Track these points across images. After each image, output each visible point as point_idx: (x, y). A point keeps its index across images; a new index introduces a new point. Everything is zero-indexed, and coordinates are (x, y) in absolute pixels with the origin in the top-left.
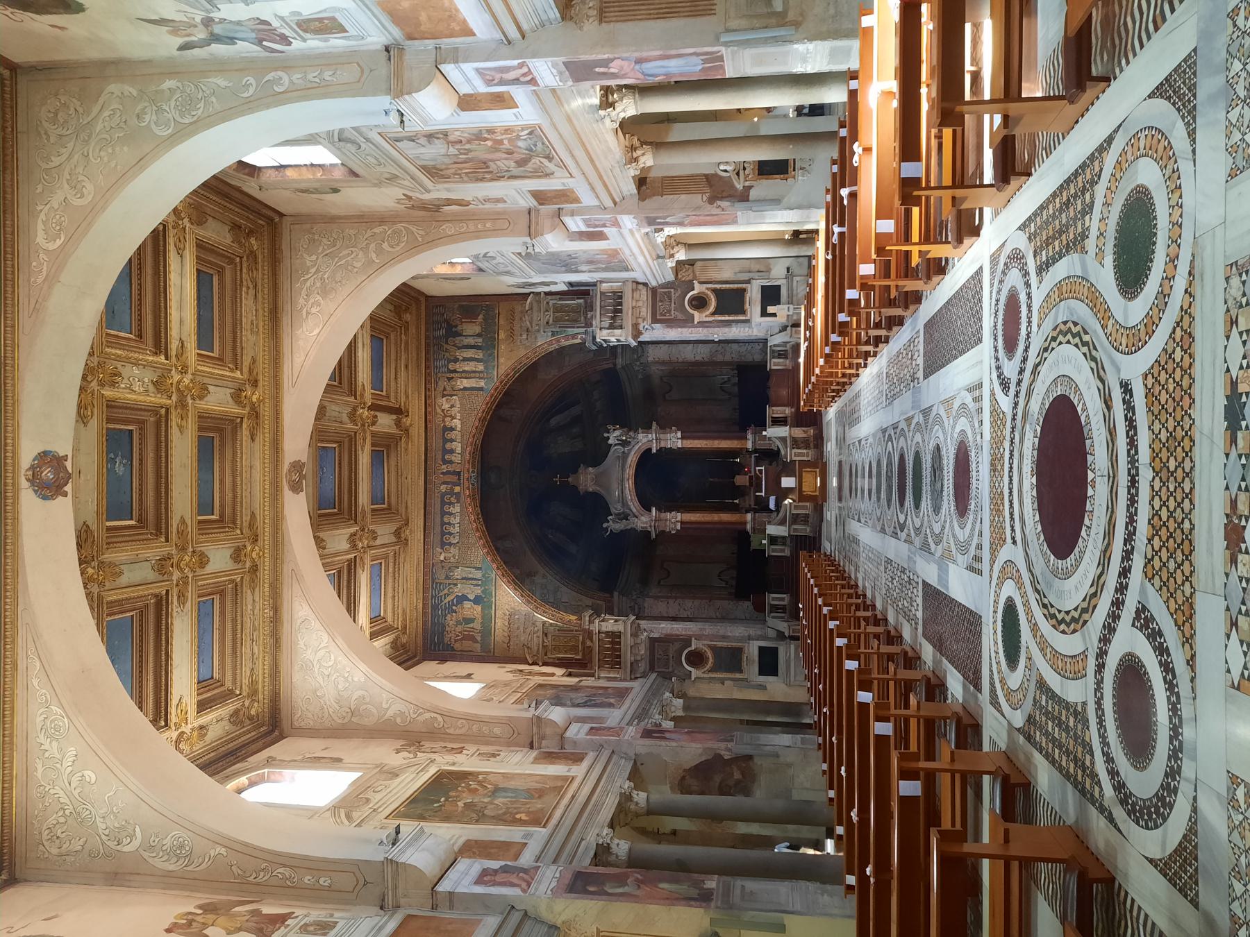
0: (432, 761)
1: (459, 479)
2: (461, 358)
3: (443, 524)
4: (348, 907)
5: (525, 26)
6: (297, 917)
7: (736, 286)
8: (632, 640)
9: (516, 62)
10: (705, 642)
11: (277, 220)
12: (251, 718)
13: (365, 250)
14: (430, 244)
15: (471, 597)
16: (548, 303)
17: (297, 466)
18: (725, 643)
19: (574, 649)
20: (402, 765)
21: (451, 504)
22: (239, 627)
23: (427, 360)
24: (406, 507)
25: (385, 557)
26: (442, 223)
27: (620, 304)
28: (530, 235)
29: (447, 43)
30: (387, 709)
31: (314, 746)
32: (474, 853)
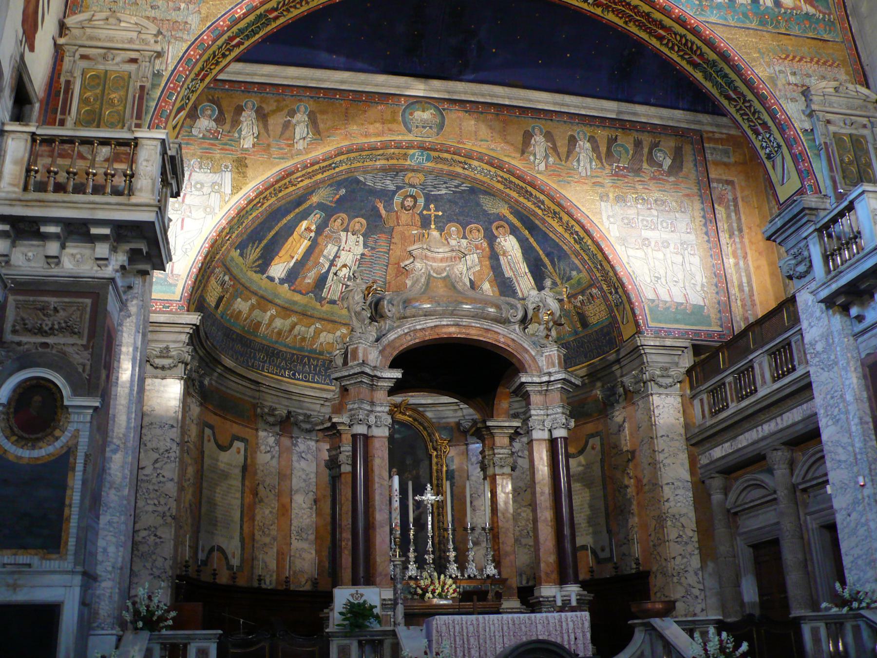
8: (106, 231)
10: (84, 440)
16: (865, 126)
18: (76, 497)
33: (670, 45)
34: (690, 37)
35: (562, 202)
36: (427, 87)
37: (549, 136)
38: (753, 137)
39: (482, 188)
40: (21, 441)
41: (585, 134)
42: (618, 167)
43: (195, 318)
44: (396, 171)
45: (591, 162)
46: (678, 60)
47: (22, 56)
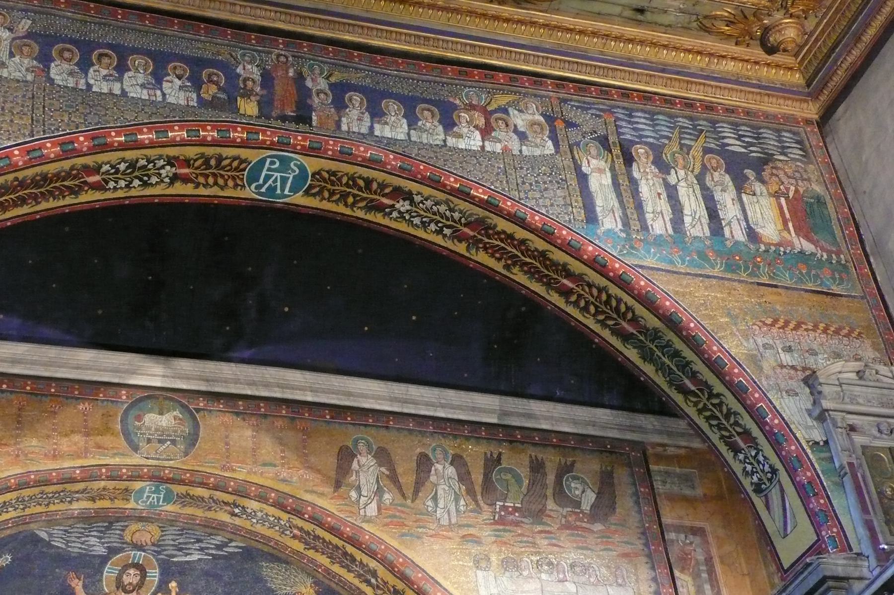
1: (284, 118)
2: (672, 179)
21: (197, 84)
23: (647, 97)
33: (582, 304)
34: (614, 290)
35: (409, 572)
36: (169, 372)
37: (383, 456)
38: (729, 456)
39: (266, 549)
41: (445, 452)
42: (504, 508)
45: (457, 500)
46: (596, 328)
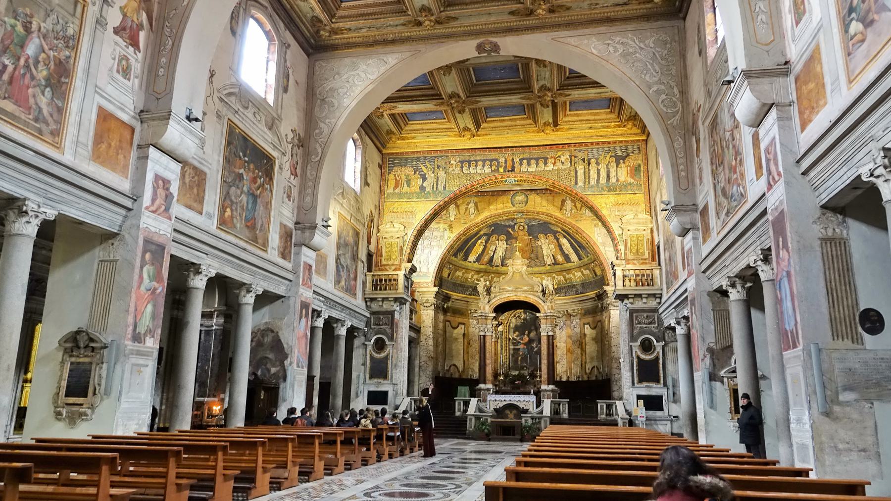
0: (284, 154)
1: (509, 171)
2: (599, 168)
3: (476, 161)
4: (144, 88)
5: (812, 174)
6: (136, 54)
7: (662, 375)
9: (781, 169)
11: (681, 15)
12: (318, 32)
13: (660, 82)
14: (666, 130)
15: (425, 184)
17: (496, 48)
19: (389, 258)
20: (280, 132)
21: (491, 166)
22: (377, 17)
23: (598, 143)
24: (486, 135)
25: (449, 122)
26: (683, 137)
27: (643, 285)
28: (675, 206)
29: (794, 111)
30: (325, 123)
31: (299, 73)
32: (193, 178)
37: (573, 201)
40: (377, 353)
43: (436, 289)
44: (513, 219)
47: (368, 250)
